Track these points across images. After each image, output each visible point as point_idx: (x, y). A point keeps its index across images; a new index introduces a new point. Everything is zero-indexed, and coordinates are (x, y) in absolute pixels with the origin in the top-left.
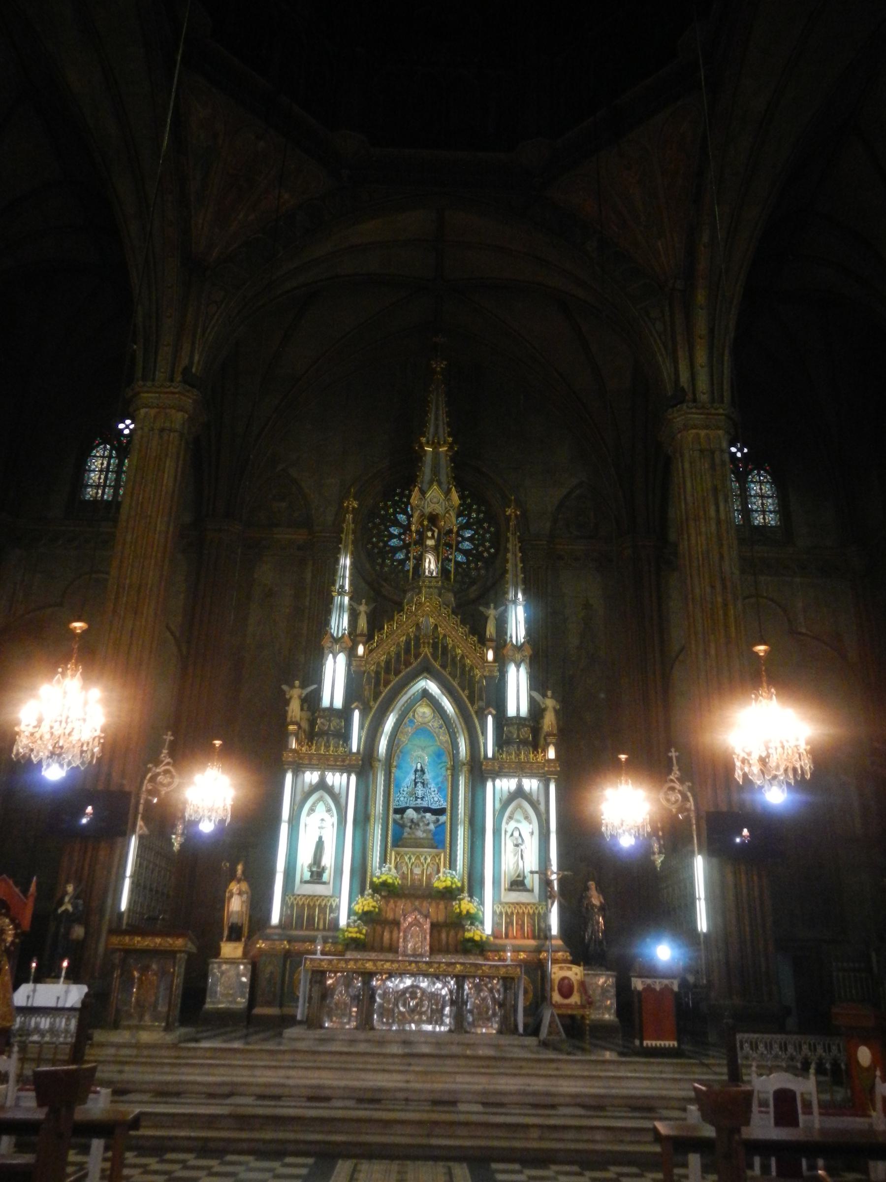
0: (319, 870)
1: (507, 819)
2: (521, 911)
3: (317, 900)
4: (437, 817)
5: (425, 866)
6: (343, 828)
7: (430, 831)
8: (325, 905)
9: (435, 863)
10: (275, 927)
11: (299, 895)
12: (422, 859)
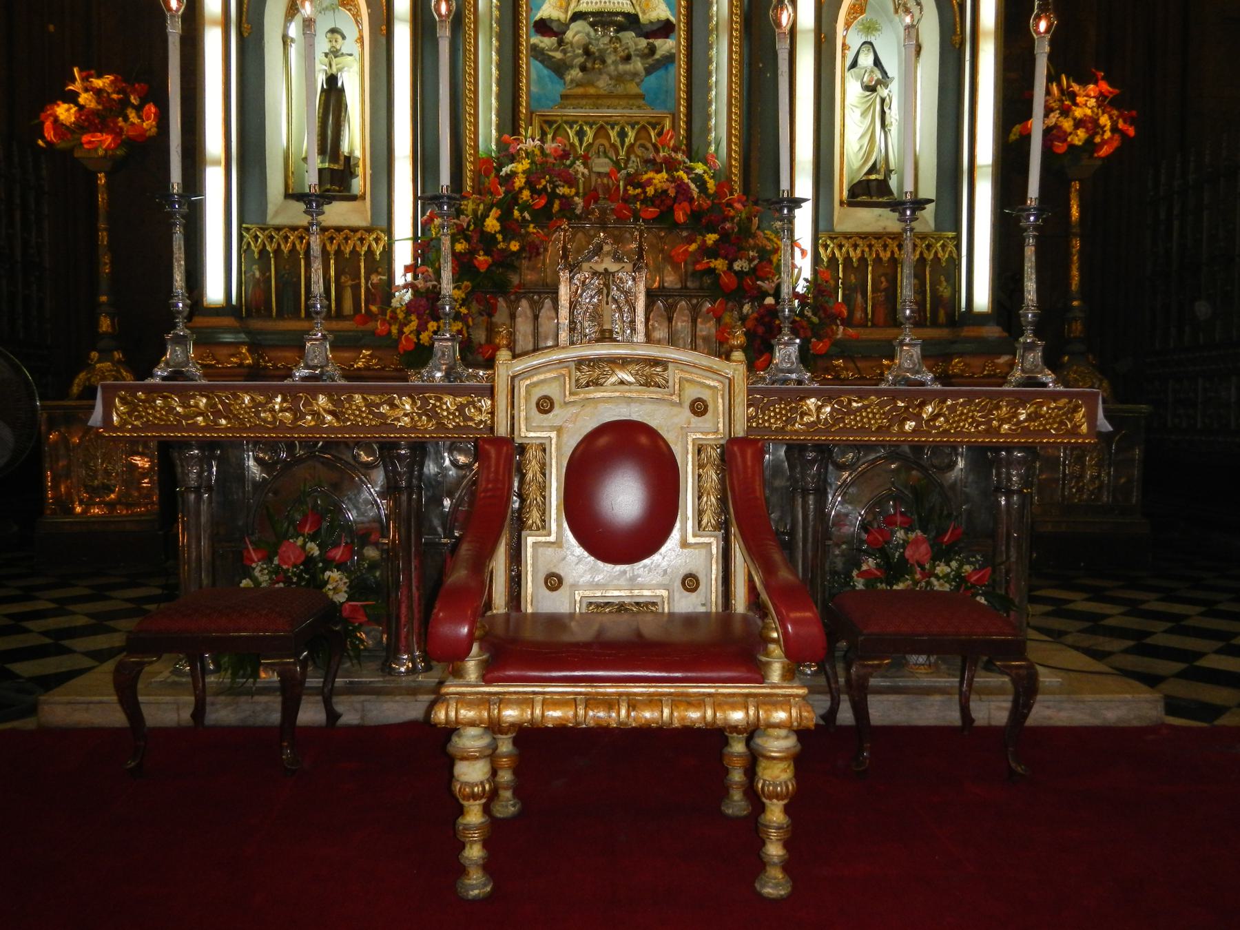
2: (885, 256)
4: (651, 41)
5: (622, 154)
6: (384, 40)
7: (635, 74)
8: (354, 252)
9: (649, 146)
10: (216, 311)
11: (278, 229)
12: (613, 134)
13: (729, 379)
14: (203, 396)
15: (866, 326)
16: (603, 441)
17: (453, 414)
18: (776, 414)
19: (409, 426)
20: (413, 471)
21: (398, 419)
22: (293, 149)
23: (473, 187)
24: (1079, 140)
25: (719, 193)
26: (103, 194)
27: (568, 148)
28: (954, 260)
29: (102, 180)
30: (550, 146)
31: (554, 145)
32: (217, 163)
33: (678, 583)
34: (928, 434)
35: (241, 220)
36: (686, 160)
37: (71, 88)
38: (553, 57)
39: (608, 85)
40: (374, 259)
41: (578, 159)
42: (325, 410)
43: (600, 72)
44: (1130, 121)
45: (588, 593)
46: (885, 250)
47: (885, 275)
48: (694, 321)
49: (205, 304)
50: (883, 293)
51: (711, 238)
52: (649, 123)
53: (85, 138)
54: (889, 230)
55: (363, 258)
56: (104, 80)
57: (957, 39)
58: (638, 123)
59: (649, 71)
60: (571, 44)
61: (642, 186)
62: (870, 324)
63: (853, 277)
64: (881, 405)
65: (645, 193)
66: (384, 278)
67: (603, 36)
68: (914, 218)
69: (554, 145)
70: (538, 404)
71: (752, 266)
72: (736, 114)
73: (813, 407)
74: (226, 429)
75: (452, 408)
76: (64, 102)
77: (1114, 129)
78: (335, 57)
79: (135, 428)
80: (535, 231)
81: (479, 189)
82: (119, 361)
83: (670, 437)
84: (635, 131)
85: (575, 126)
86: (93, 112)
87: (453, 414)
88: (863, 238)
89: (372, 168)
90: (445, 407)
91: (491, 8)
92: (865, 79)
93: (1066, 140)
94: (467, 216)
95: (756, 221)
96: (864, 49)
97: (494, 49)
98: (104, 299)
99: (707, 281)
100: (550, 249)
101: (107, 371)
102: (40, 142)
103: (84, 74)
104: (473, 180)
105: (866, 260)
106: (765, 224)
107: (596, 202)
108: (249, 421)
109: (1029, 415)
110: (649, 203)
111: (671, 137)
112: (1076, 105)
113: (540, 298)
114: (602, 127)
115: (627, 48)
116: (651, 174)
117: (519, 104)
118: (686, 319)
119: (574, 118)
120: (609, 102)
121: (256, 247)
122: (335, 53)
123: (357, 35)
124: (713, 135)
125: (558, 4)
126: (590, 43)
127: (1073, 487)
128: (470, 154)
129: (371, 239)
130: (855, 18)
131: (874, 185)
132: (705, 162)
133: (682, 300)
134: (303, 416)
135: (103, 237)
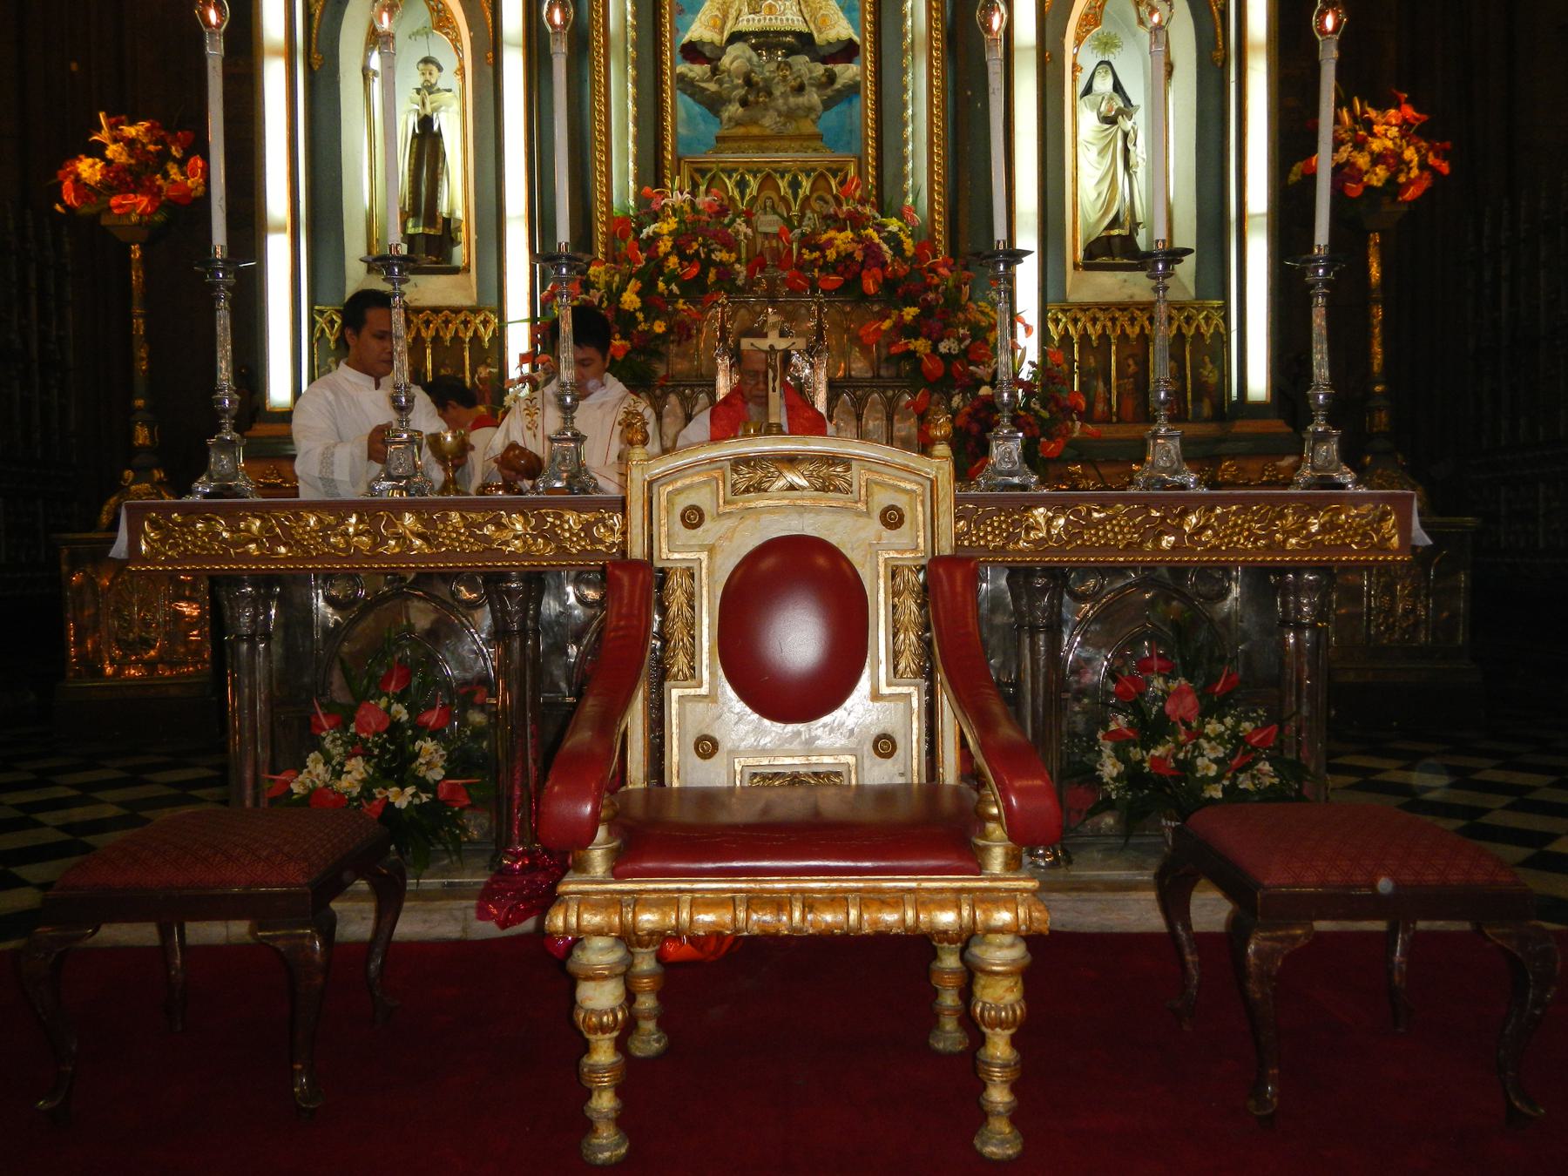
0: (432, 232)
1: (1080, 25)
2: (1133, 332)
3: (427, 323)
4: (829, 66)
5: (795, 210)
6: (490, 71)
7: (811, 109)
8: (457, 339)
9: (829, 198)
12: (783, 185)
13: (932, 481)
14: (256, 517)
15: (1109, 422)
16: (768, 563)
17: (577, 535)
18: (994, 528)
19: (521, 551)
20: (527, 610)
21: (507, 543)
22: (378, 210)
23: (606, 254)
24: (1379, 180)
25: (919, 256)
26: (137, 272)
27: (726, 202)
28: (1222, 335)
29: (136, 252)
30: (702, 200)
31: (707, 199)
32: (280, 229)
33: (868, 746)
34: (1192, 551)
35: (312, 302)
36: (877, 215)
37: (96, 138)
38: (707, 89)
39: (776, 123)
40: (482, 347)
41: (739, 216)
42: (412, 533)
43: (766, 108)
44: (1443, 154)
45: (751, 761)
46: (1132, 325)
47: (1132, 356)
48: (890, 419)
49: (268, 407)
50: (1131, 380)
51: (910, 313)
52: (829, 170)
53: (114, 201)
54: (1137, 298)
55: (467, 346)
56: (138, 128)
57: (1219, 55)
58: (814, 170)
59: (828, 104)
60: (729, 71)
61: (822, 248)
62: (1114, 419)
63: (1092, 360)
64: (1131, 515)
65: (824, 257)
66: (494, 370)
67: (768, 62)
68: (1168, 274)
69: (707, 199)
70: (683, 516)
71: (962, 347)
72: (939, 155)
73: (1041, 520)
74: (287, 559)
75: (576, 528)
76: (88, 156)
77: (1423, 166)
78: (429, 94)
79: (170, 560)
80: (685, 307)
81: (613, 257)
82: (160, 482)
83: (854, 556)
84: (811, 180)
85: (735, 175)
86: (125, 169)
87: (577, 535)
88: (1104, 310)
89: (477, 233)
90: (566, 527)
91: (626, 27)
92: (1102, 109)
93: (1361, 180)
94: (599, 290)
95: (966, 289)
96: (1100, 70)
97: (630, 79)
98: (140, 403)
99: (907, 367)
100: (705, 330)
101: (145, 494)
102: (58, 207)
103: (113, 120)
104: (606, 245)
105: (1108, 338)
106: (978, 294)
107: (762, 271)
108: (316, 548)
109: (1322, 526)
110: (830, 270)
111: (857, 187)
112: (1374, 135)
113: (693, 392)
114: (769, 175)
115: (798, 77)
116: (832, 234)
117: (664, 148)
118: (880, 415)
119: (734, 166)
120: (777, 144)
121: (331, 335)
122: (429, 89)
123: (457, 65)
124: (910, 182)
125: (711, 23)
126: (752, 71)
127: (1381, 624)
128: (602, 213)
129: (477, 321)
130: (1088, 31)
131: (1117, 240)
132: (901, 217)
133: (873, 392)
134: (384, 541)
135: (139, 326)
